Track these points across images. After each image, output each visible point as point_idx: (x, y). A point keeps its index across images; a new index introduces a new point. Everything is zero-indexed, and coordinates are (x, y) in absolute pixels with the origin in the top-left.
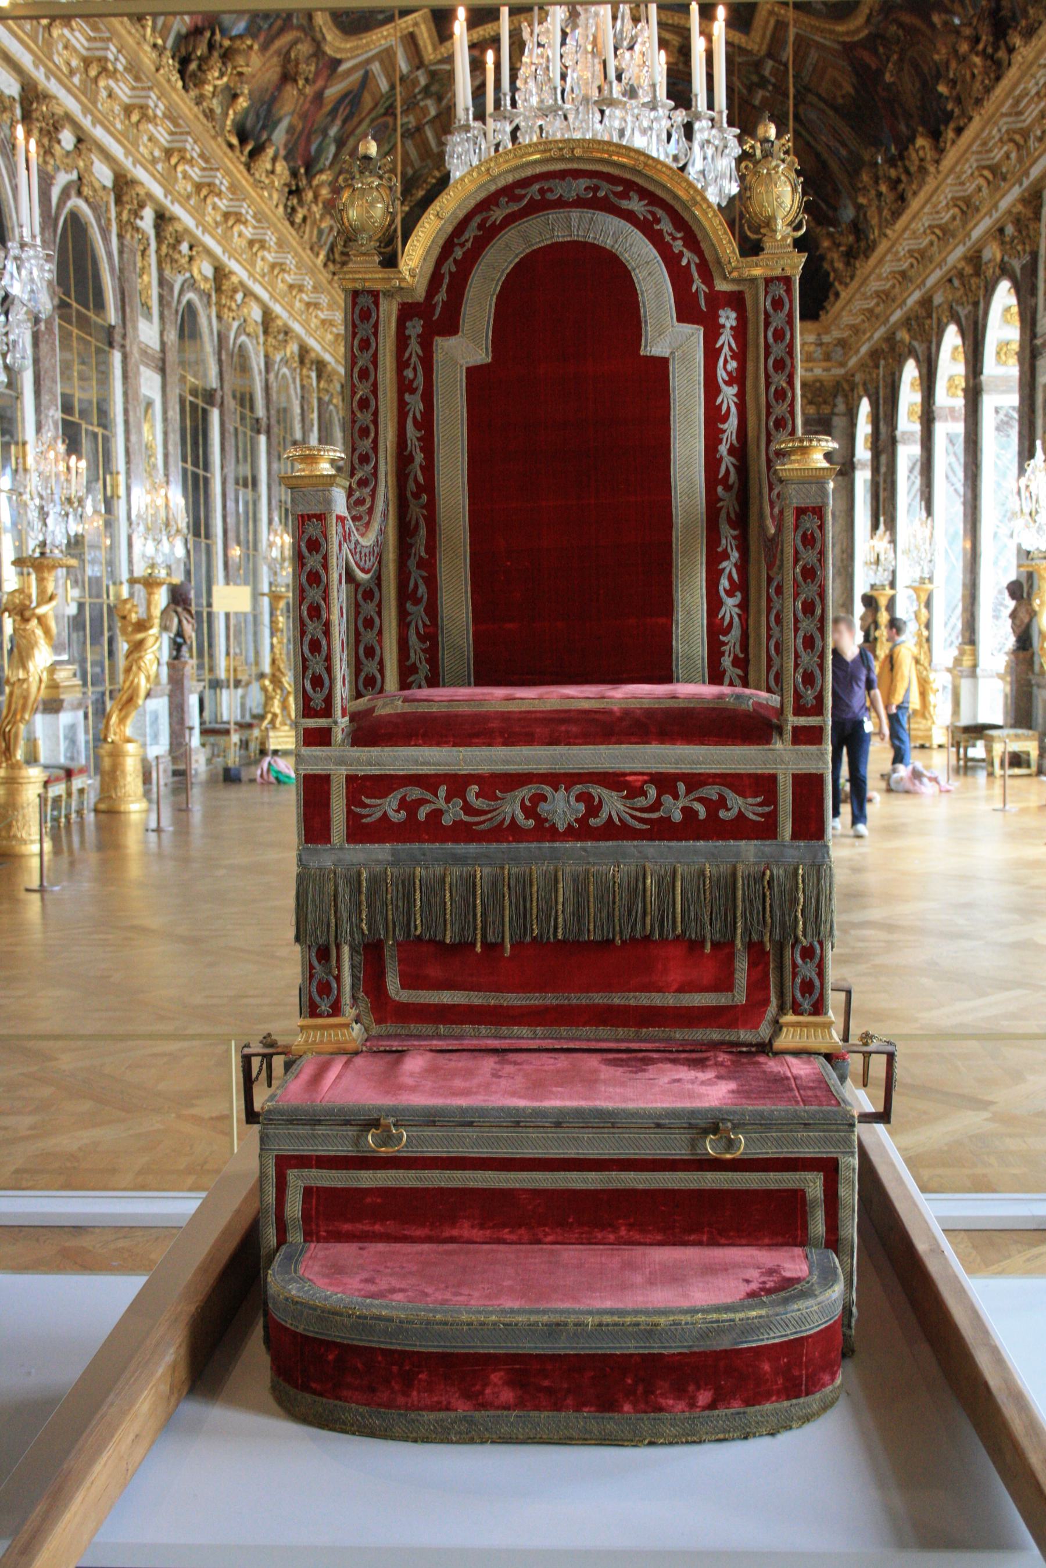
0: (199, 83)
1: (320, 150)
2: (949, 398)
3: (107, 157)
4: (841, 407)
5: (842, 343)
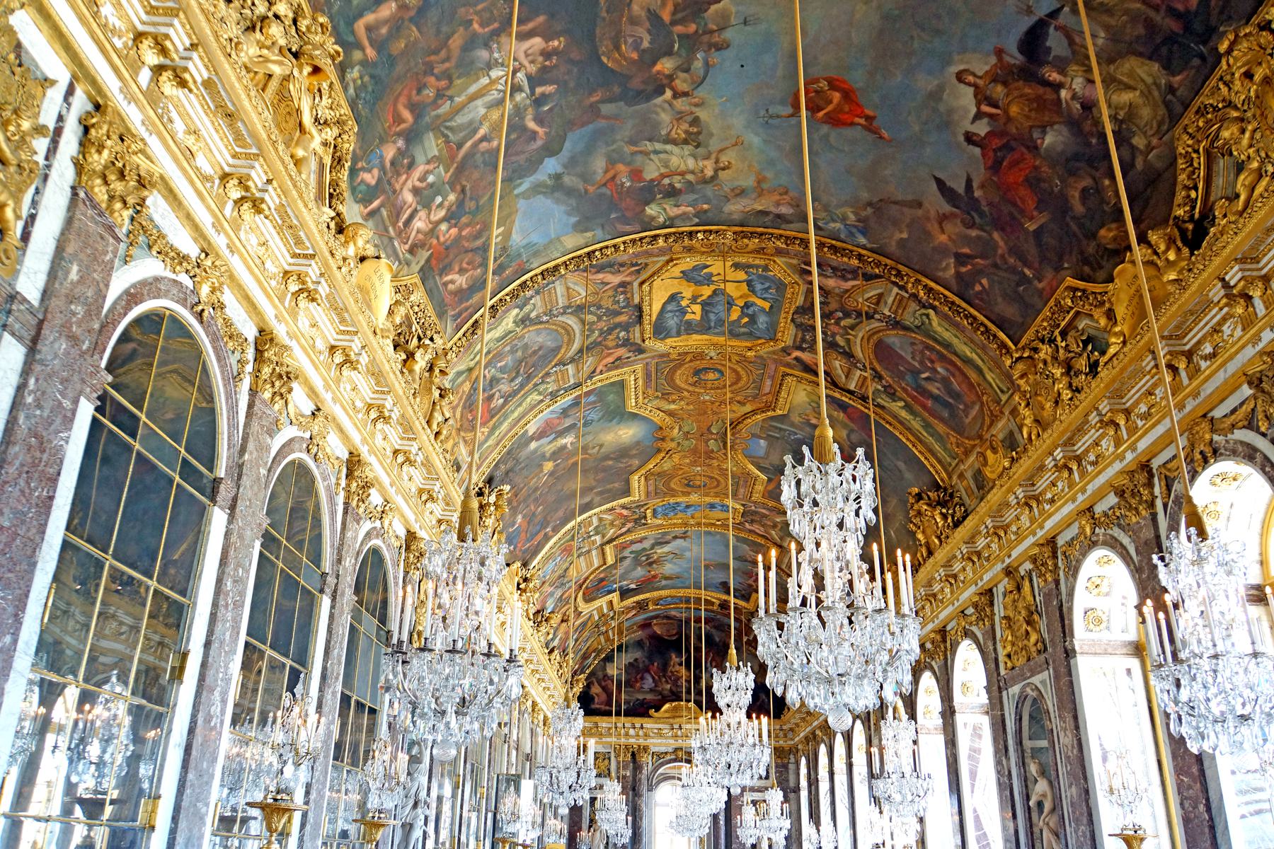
2: (840, 764)
4: (792, 760)
5: (791, 730)
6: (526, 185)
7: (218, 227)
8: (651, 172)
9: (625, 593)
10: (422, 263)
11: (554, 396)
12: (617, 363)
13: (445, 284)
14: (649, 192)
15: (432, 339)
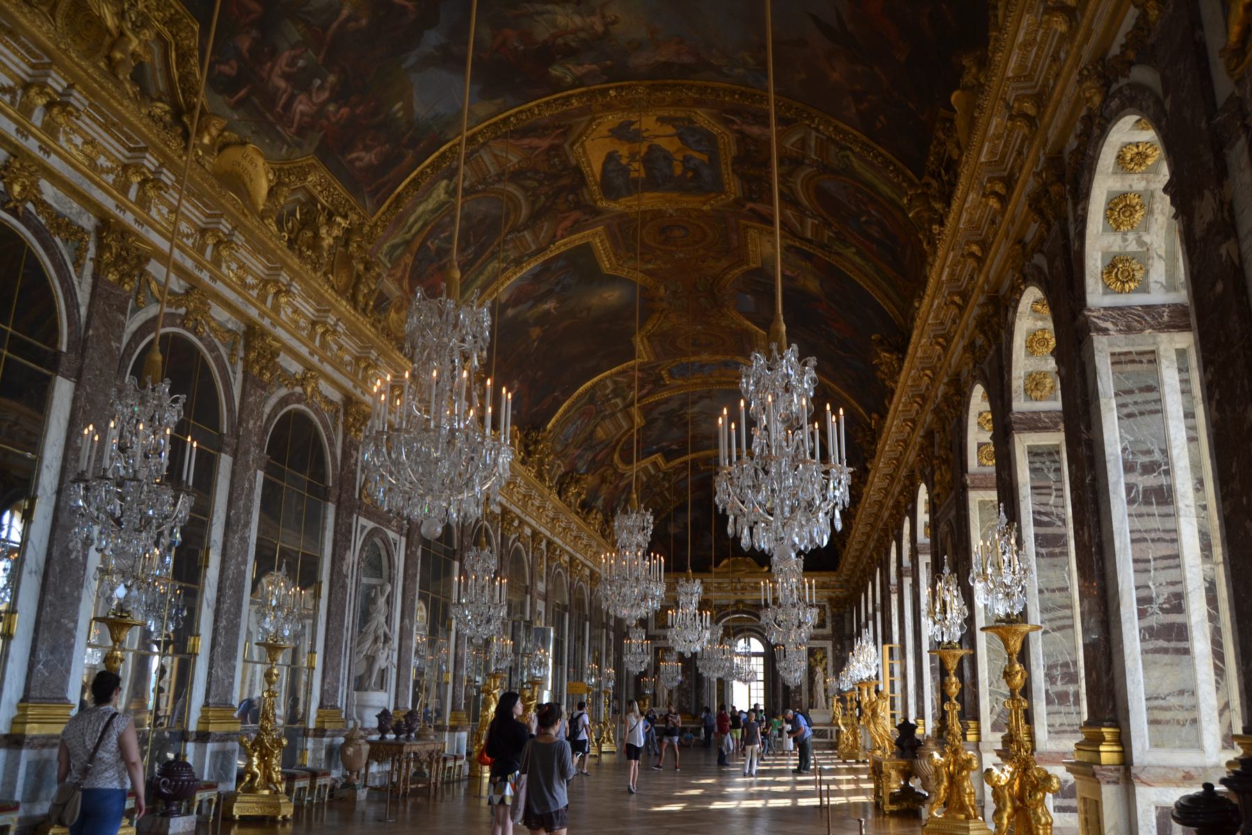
3: (530, 525)
6: (412, 59)
7: (23, 131)
8: (542, 32)
9: (669, 455)
10: (316, 144)
11: (518, 262)
12: (576, 228)
13: (352, 162)
14: (548, 53)
15: (345, 217)
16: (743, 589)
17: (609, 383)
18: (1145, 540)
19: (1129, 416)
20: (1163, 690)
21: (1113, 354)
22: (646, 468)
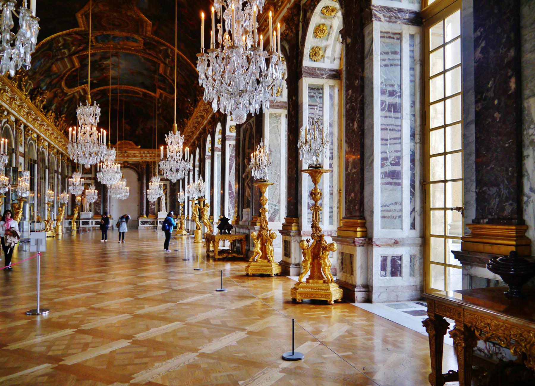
0: (35, 99)
1: (63, 110)
3: (14, 115)
16: (128, 156)
17: (61, 40)
18: (387, 129)
19: (386, 65)
20: (388, 203)
21: (381, 32)
22: (79, 91)
